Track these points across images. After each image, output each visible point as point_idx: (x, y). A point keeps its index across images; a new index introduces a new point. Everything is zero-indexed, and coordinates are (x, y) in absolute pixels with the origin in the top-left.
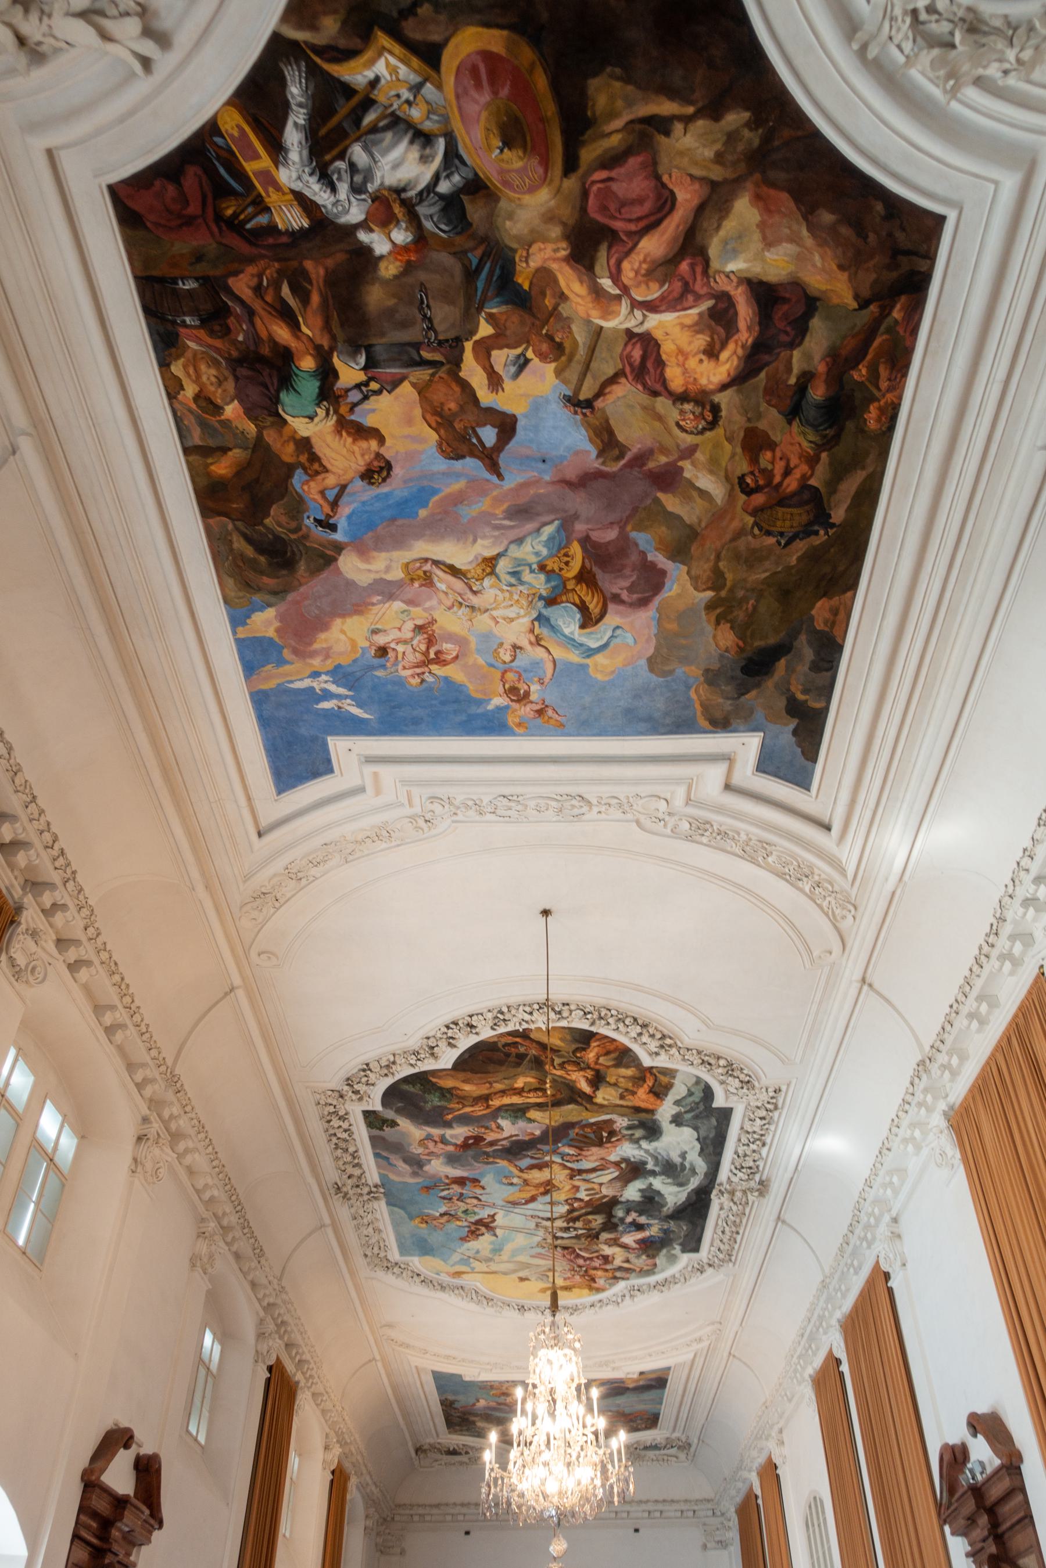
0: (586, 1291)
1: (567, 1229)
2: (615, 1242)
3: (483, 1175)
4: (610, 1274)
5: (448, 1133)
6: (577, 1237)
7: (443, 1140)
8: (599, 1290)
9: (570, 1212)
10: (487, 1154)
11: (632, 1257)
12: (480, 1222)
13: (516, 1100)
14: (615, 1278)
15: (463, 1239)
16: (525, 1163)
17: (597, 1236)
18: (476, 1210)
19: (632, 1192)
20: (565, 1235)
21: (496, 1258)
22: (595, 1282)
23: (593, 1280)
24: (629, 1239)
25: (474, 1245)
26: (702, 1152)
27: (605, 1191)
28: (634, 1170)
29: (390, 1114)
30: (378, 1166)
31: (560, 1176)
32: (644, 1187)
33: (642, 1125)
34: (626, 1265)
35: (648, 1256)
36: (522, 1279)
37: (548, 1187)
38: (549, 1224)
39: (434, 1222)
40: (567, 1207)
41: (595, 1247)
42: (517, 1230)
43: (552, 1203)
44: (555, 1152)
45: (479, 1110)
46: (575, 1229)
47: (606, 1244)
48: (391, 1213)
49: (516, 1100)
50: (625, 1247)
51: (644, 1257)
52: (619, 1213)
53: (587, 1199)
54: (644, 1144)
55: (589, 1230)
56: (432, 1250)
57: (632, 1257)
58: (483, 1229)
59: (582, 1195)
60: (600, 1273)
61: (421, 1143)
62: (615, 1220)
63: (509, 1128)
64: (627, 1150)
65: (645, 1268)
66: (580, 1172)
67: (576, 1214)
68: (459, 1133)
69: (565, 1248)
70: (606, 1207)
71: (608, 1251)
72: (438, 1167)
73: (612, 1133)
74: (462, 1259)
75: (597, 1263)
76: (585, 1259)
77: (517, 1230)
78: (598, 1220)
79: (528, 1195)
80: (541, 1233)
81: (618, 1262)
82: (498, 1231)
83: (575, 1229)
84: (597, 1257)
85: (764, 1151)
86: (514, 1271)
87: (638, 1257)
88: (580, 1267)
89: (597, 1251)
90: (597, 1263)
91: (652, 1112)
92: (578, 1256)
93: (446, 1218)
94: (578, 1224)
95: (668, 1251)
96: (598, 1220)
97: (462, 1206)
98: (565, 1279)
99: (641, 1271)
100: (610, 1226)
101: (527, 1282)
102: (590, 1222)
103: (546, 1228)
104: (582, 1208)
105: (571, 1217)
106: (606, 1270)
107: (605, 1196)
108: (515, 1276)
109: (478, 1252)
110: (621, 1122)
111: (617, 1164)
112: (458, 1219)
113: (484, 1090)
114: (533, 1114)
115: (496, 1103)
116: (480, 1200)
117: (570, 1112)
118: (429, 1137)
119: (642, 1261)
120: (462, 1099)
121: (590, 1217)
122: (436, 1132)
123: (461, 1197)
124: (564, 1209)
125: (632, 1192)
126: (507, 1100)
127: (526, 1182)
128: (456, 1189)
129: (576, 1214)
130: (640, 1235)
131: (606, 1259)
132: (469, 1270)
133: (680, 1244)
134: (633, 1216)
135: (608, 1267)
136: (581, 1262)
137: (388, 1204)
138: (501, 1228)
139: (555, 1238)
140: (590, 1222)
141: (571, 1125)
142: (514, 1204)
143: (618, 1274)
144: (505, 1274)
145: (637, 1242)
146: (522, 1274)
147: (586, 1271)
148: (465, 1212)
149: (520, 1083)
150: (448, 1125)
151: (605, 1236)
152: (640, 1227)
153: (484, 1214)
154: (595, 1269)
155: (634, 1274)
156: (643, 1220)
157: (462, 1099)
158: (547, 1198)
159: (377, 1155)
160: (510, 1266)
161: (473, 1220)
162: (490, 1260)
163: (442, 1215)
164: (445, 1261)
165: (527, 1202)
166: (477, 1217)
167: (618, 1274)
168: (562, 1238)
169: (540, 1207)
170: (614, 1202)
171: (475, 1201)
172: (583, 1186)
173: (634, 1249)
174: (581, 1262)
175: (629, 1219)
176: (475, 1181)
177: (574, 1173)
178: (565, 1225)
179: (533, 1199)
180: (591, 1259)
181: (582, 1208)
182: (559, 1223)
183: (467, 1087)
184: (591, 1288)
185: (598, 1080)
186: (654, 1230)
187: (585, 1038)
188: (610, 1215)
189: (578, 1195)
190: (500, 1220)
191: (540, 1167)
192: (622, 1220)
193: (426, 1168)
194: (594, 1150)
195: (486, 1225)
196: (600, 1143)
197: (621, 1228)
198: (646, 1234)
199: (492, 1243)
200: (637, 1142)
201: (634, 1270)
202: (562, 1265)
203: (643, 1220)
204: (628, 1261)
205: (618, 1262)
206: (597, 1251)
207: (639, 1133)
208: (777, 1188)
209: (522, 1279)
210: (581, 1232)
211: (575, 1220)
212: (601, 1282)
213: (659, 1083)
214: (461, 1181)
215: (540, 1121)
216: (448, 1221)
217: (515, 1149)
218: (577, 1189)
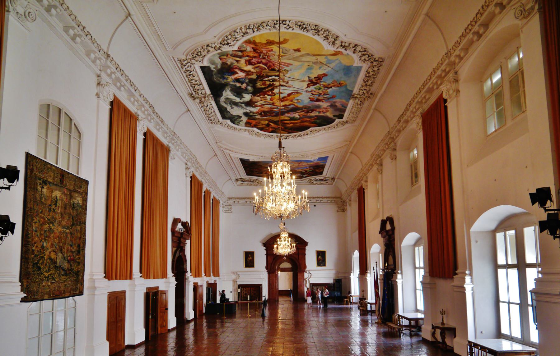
0: (257, 41)
1: (274, 80)
2: (248, 73)
3: (309, 102)
4: (245, 54)
5: (317, 114)
6: (268, 76)
7: (320, 112)
8: (248, 42)
9: (273, 89)
10: (305, 108)
11: (235, 63)
12: (314, 84)
13: (293, 122)
14: (242, 51)
15: (325, 75)
16: (292, 106)
17: (258, 77)
18: (315, 90)
19: (247, 97)
20: (274, 77)
21: (311, 64)
22: (253, 48)
23: (255, 50)
24: (241, 75)
25: (321, 72)
26: (226, 108)
27: (259, 98)
28: (250, 104)
29: (334, 118)
30: (347, 105)
31: (277, 103)
32: (243, 99)
33: (251, 116)
34: (238, 59)
35: (227, 64)
36: (298, 50)
37: (283, 99)
38: (282, 83)
39: (336, 84)
40: (274, 92)
41: (257, 70)
42: (297, 80)
43: (280, 93)
44: (280, 109)
45: (305, 119)
46: (269, 81)
47: (252, 72)
48: (353, 87)
49: (293, 122)
50: (242, 71)
51: (229, 63)
52: (250, 88)
53: (266, 96)
54: (248, 111)
55: (262, 80)
56: (344, 69)
57: (235, 63)
58: (314, 80)
59: (269, 97)
60: (252, 55)
61: (327, 111)
62: (251, 85)
63: (296, 115)
64: (254, 110)
65: (225, 57)
66: (270, 104)
67: (270, 88)
68: (313, 114)
69: (274, 70)
70: (256, 92)
71: (249, 68)
72: (324, 105)
73: (261, 114)
74: (330, 64)
75: (254, 60)
76: (261, 62)
77: (297, 80)
78: (259, 85)
79: (291, 96)
80: (286, 79)
81: (243, 61)
82: (307, 79)
83: (269, 81)
84: (255, 64)
85: (203, 109)
86: (302, 56)
87: (232, 64)
88: (264, 58)
89: (256, 67)
90: (254, 60)
91: (249, 119)
92: (266, 64)
93: (330, 86)
94: (268, 83)
95: (217, 67)
96: (259, 85)
97: (320, 91)
98: (272, 50)
99: (227, 55)
100: (253, 82)
101: (296, 48)
102: (263, 84)
103: (284, 81)
104: (268, 91)
105: (272, 87)
106: (248, 56)
107: (258, 96)
108: (303, 52)
109: (320, 68)
110: (258, 117)
111: (256, 106)
112: (324, 85)
113: (302, 124)
114: (288, 118)
115: (299, 121)
116: (312, 94)
117: (275, 119)
118: (324, 113)
119: (230, 61)
120: (310, 122)
121: (263, 87)
122: (322, 114)
123: (320, 94)
124: (276, 91)
125: (247, 97)
126: (296, 121)
127: (292, 101)
128: (320, 98)
129: (270, 88)
130: (236, 76)
131: (249, 63)
132: (329, 56)
133: (212, 71)
134: (244, 85)
135: (247, 58)
136: (264, 61)
137: (352, 91)
138: (305, 81)
139: (278, 76)
140: (263, 84)
141: (274, 116)
142: (297, 93)
143: (240, 53)
144: (308, 54)
145: (235, 73)
146: (298, 54)
147: (260, 56)
148: (320, 89)
149: (291, 125)
150: (316, 116)
151: (254, 77)
152: (237, 80)
153: (312, 88)
154: (255, 57)
155: (231, 53)
156: (238, 85)
157: (310, 122)
158: (282, 96)
159: (346, 108)
160: (304, 59)
161: (318, 85)
162: (315, 63)
163: (331, 87)
164: (340, 62)
165: (292, 93)
166: (315, 86)
167: (240, 53)
168: (275, 76)
169: (286, 91)
170: (254, 93)
171: (314, 93)
172: (268, 100)
173: (236, 68)
174: (264, 61)
175: (244, 85)
176: (312, 100)
177: (273, 104)
178: (275, 83)
179: (289, 95)
180: (258, 63)
181: (268, 91)
182: (277, 84)
183: (307, 124)
184: (254, 43)
185: (268, 125)
186: (230, 79)
187: (272, 132)
188: (254, 87)
189: (270, 97)
190: (305, 85)
191: (286, 105)
192: (248, 85)
193: (330, 104)
194: (266, 110)
195: (312, 82)
196: (264, 112)
197: (247, 81)
198: (233, 77)
199: (311, 73)
200: (251, 112)
201: (231, 55)
202: (274, 59)
203: (238, 85)
204: (237, 61)
205: (243, 61)
206: (256, 67)
207: (251, 114)
208: (188, 100)
209: (298, 50)
210: (266, 79)
211: (270, 85)
212: (249, 48)
213: (248, 124)
214: (318, 100)
215: (286, 116)
216: (329, 84)
217: (295, 109)
218: (271, 99)
